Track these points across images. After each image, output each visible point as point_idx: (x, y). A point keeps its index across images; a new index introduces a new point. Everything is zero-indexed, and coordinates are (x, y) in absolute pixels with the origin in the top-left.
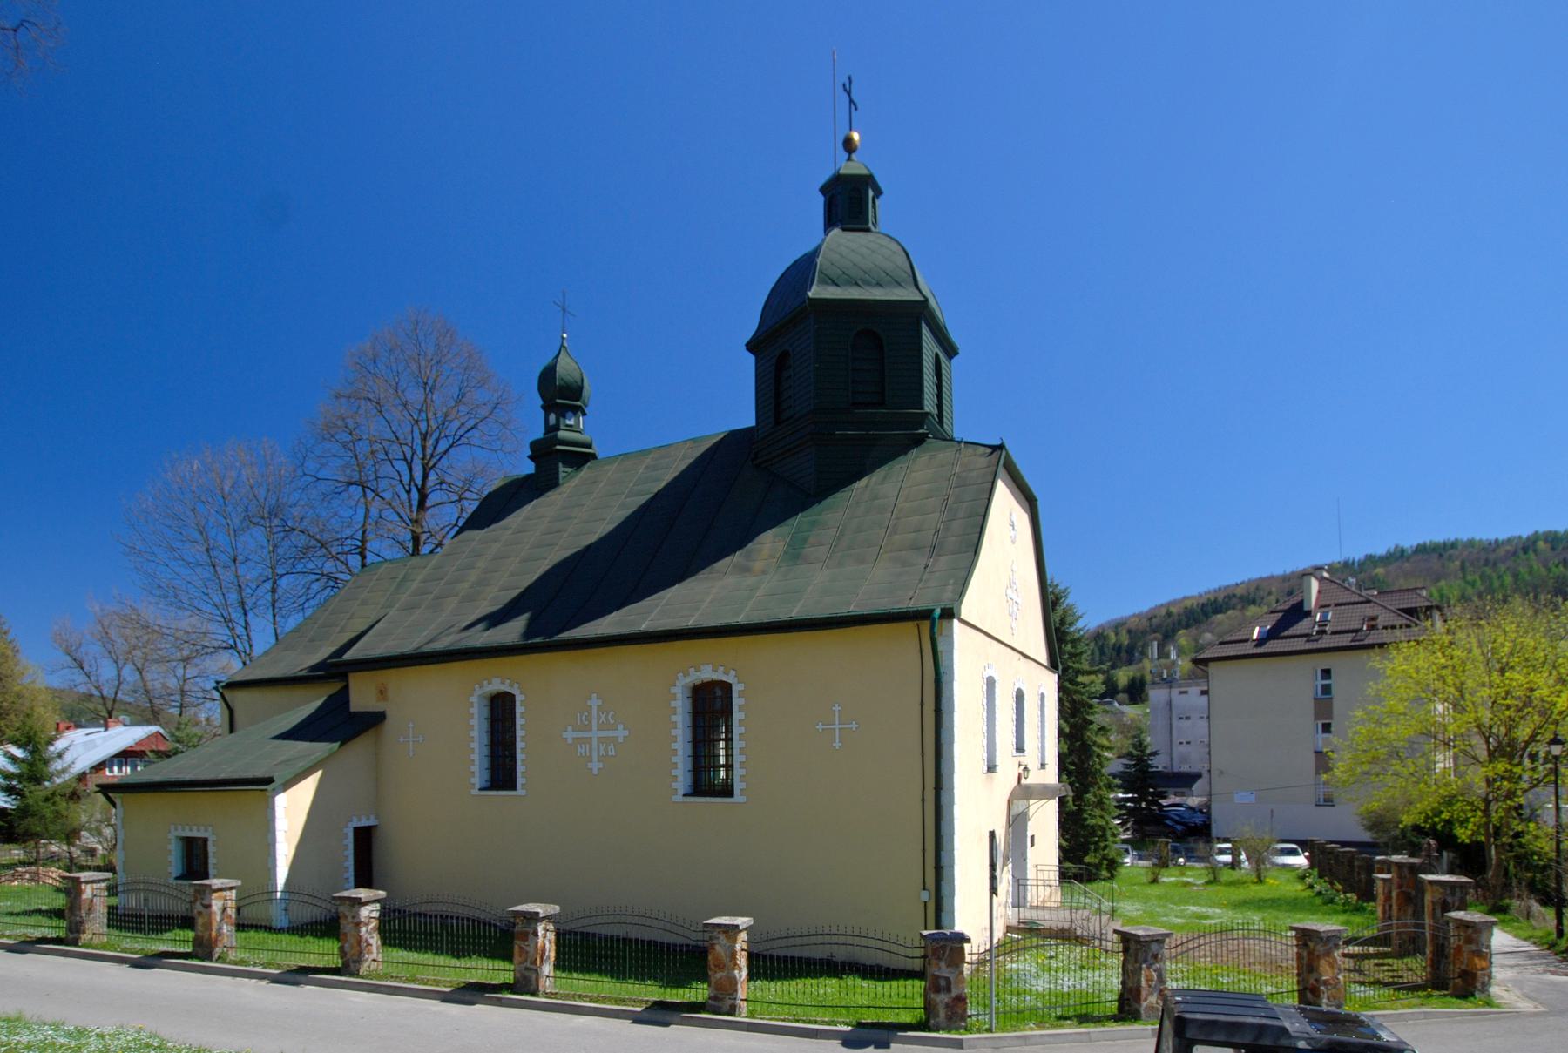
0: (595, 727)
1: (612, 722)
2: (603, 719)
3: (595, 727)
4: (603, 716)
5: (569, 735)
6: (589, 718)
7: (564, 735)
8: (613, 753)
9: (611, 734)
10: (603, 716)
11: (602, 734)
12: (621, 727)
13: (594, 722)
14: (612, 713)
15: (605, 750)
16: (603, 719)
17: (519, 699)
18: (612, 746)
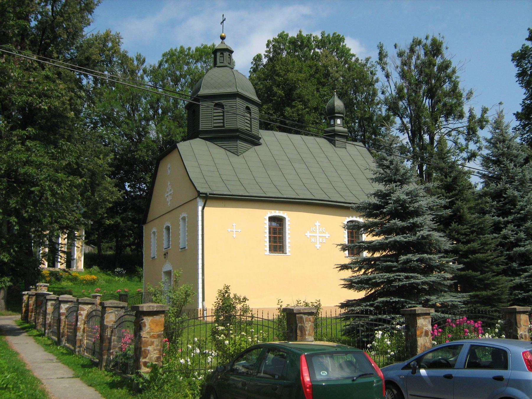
0: (318, 232)
1: (324, 231)
2: (321, 230)
3: (318, 232)
4: (321, 229)
5: (308, 234)
6: (315, 229)
7: (306, 234)
8: (324, 241)
9: (324, 235)
10: (321, 229)
11: (320, 235)
12: (327, 233)
13: (318, 230)
14: (324, 228)
15: (322, 240)
16: (321, 230)
17: (287, 219)
18: (324, 239)
